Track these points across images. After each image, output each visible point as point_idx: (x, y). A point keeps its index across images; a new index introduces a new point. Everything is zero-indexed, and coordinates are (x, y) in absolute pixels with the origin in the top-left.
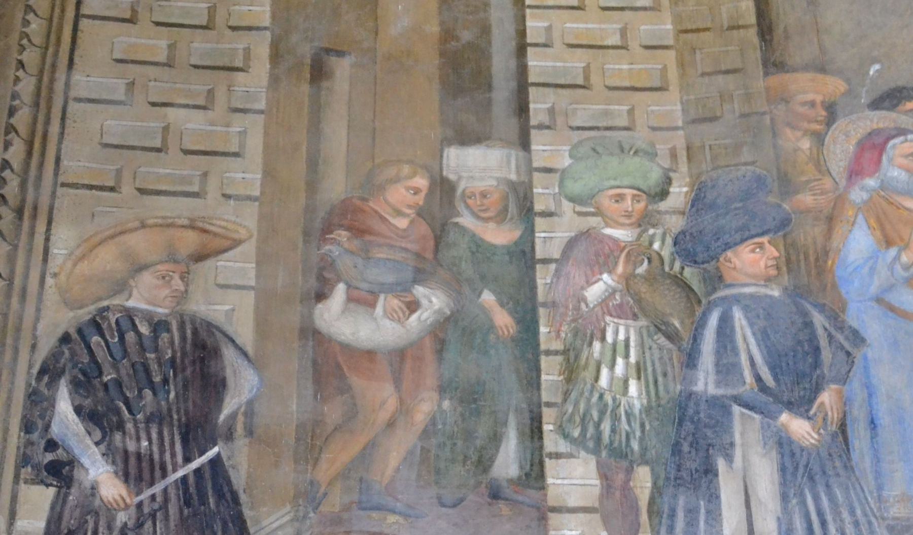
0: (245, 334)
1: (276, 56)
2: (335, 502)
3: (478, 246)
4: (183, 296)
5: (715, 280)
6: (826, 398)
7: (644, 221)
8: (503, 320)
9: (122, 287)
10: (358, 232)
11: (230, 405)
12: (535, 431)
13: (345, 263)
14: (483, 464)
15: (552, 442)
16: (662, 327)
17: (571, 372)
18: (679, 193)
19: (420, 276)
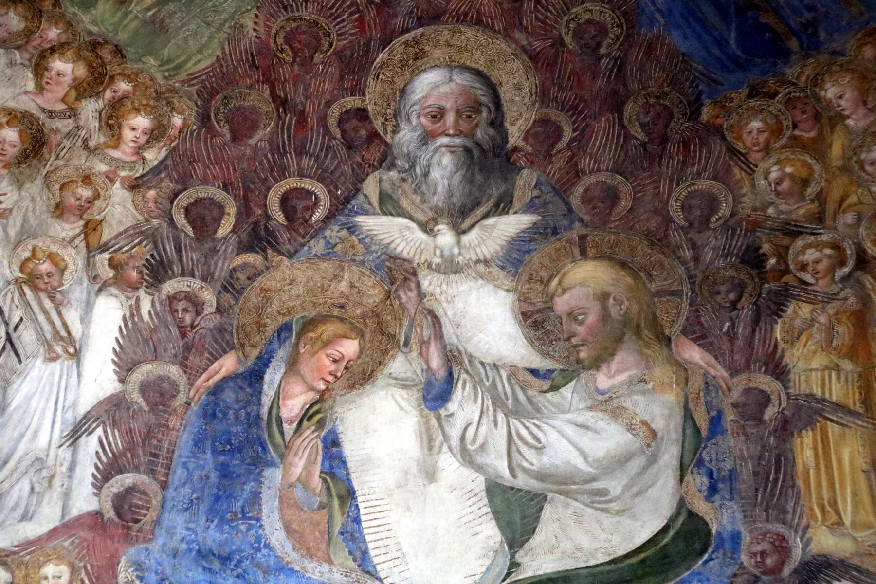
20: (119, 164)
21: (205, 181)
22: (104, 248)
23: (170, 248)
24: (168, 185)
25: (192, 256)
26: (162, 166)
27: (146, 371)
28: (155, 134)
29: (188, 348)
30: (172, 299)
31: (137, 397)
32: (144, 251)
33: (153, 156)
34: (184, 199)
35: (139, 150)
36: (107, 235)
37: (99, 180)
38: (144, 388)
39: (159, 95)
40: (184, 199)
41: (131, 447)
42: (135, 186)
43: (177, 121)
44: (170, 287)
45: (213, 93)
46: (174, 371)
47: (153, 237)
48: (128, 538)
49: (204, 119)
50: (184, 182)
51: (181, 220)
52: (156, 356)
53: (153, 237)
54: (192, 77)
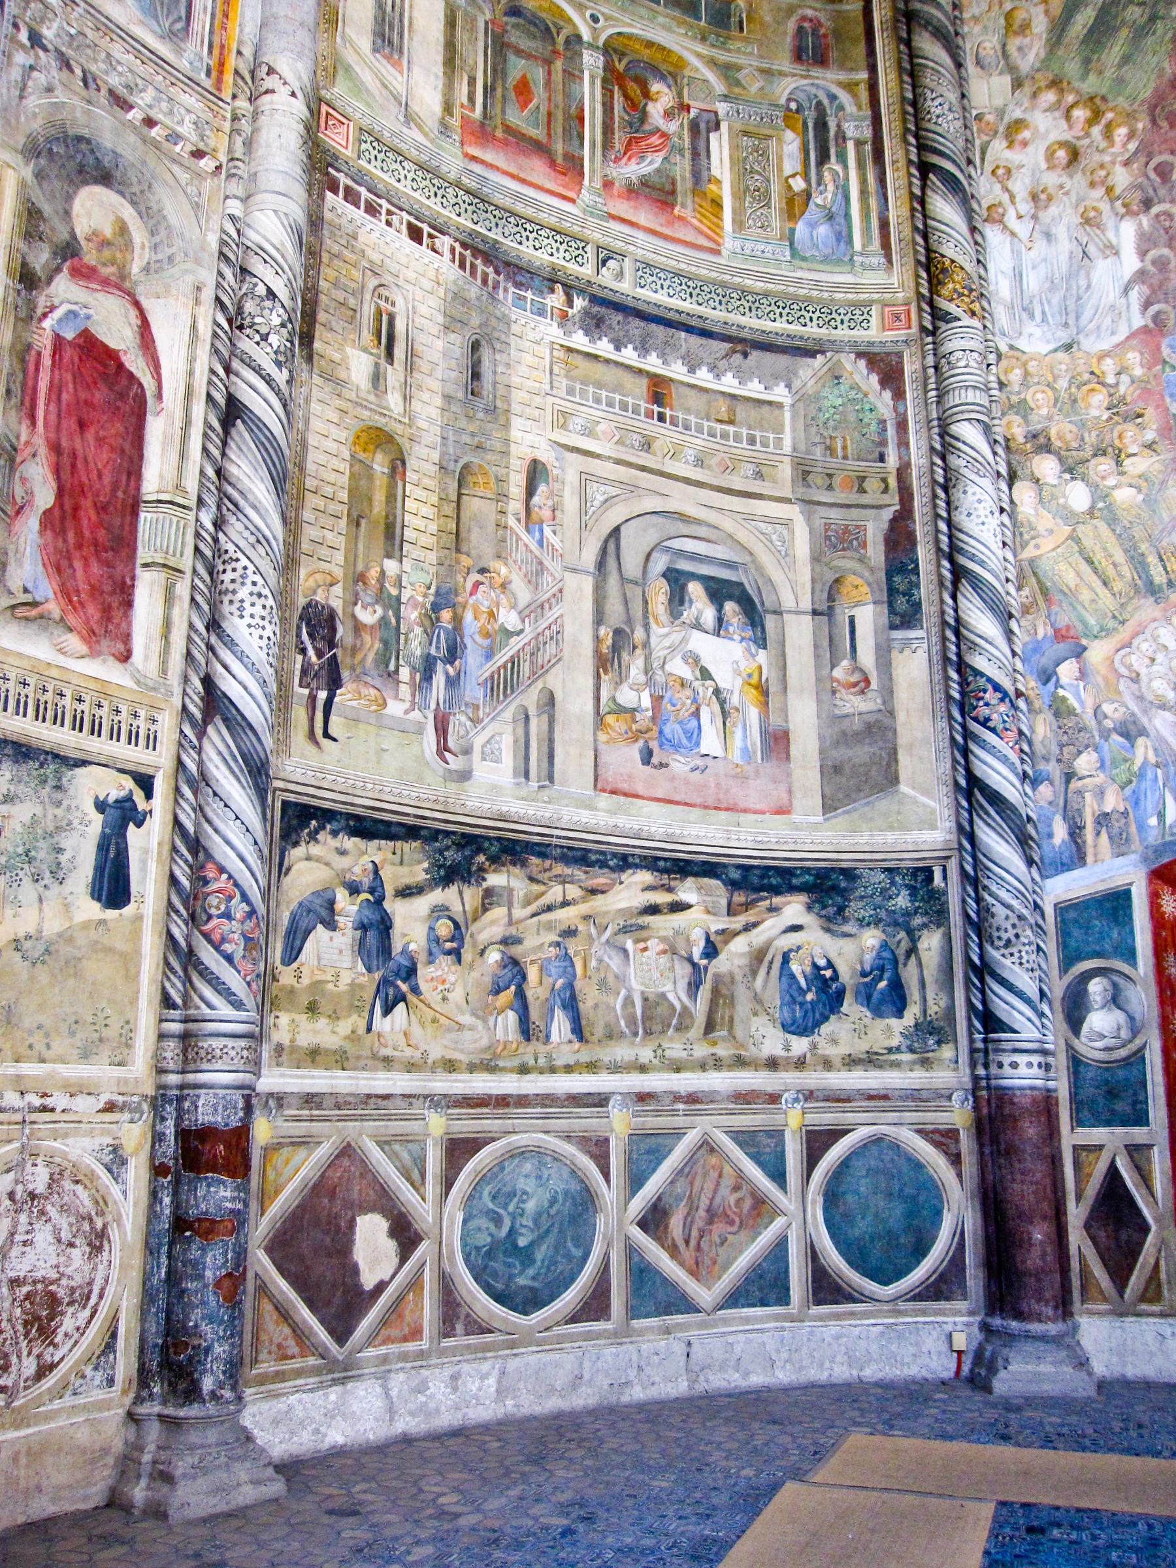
0: (340, 612)
1: (349, 515)
2: (358, 671)
3: (389, 594)
4: (327, 598)
5: (438, 619)
6: (457, 663)
7: (425, 596)
8: (393, 621)
9: (315, 593)
10: (365, 583)
11: (338, 636)
12: (398, 658)
13: (361, 594)
14: (387, 666)
15: (401, 662)
16: (425, 632)
17: (406, 640)
18: (433, 588)
19: (377, 602)
20: (1115, 155)
21: (1160, 153)
22: (1118, 198)
23: (1151, 191)
24: (1143, 160)
25: (1162, 192)
26: (1135, 153)
27: (1152, 254)
28: (1131, 136)
29: (1171, 239)
30: (1157, 216)
31: (1152, 269)
32: (1138, 195)
33: (1132, 146)
34: (1152, 164)
35: (1124, 145)
36: (1118, 191)
37: (1108, 166)
38: (1154, 263)
39: (1128, 115)
40: (1152, 164)
41: (1153, 291)
42: (1126, 164)
43: (1140, 126)
44: (1155, 210)
45: (1156, 106)
46: (1166, 251)
47: (1140, 187)
48: (1163, 335)
49: (1154, 122)
50: (1150, 157)
51: (1153, 175)
52: (1155, 245)
53: (1140, 187)
54: (1143, 101)
